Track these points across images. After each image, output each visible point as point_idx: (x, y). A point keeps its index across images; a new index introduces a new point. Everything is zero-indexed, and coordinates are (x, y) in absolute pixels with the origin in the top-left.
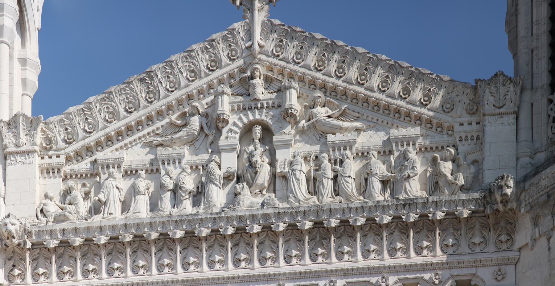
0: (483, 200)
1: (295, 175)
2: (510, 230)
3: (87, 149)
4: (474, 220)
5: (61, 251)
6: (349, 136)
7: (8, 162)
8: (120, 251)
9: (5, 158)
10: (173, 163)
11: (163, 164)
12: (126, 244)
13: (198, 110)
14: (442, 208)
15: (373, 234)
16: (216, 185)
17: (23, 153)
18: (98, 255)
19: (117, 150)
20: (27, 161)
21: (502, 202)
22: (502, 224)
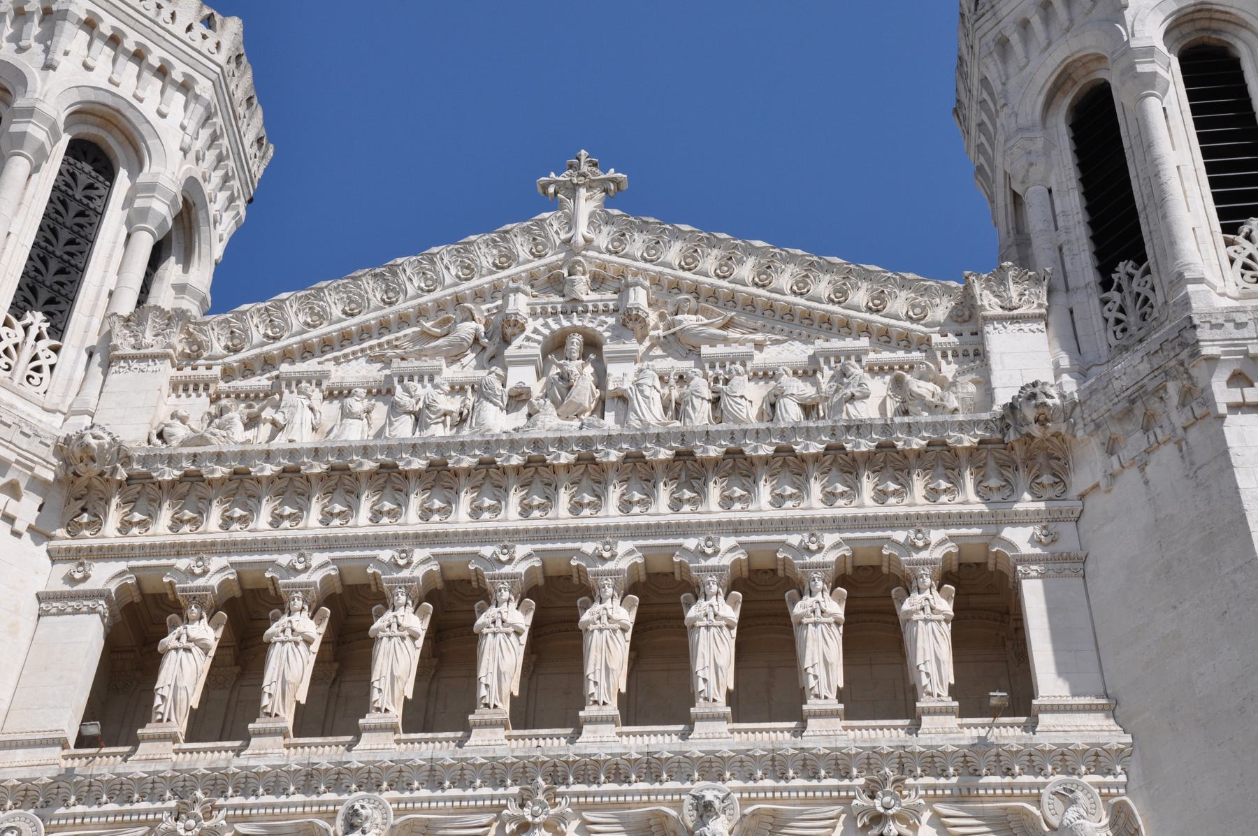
0: (998, 423)
1: (641, 392)
2: (1057, 468)
3: (266, 361)
4: (984, 455)
5: (184, 488)
7: (113, 369)
8: (300, 491)
10: (419, 381)
11: (401, 381)
12: (313, 480)
13: (472, 314)
14: (920, 432)
15: (787, 474)
16: (495, 404)
17: (144, 358)
18: (254, 497)
20: (150, 369)
21: (1037, 421)
22: (1041, 459)
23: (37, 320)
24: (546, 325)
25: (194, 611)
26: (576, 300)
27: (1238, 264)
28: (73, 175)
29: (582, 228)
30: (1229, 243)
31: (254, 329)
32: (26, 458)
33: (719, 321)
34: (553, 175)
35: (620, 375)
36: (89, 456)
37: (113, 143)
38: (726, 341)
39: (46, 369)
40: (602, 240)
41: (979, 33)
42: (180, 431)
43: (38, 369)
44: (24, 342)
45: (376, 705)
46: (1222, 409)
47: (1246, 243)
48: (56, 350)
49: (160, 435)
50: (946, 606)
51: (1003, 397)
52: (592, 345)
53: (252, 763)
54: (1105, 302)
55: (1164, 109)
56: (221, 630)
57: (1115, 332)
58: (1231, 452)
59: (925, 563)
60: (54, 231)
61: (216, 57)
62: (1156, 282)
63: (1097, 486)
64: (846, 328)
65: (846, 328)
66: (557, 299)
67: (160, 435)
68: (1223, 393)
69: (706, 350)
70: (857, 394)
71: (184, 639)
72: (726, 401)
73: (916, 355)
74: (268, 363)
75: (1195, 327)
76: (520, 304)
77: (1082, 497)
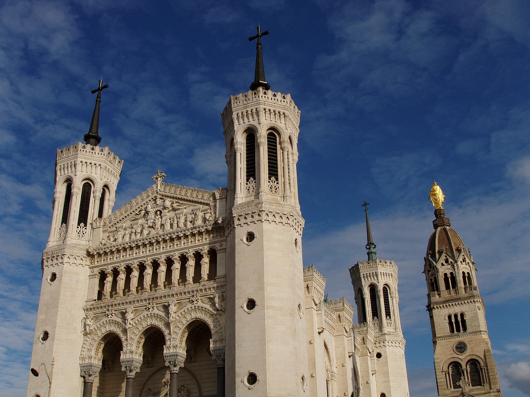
6: (181, 211)
23: (82, 224)
26: (157, 205)
27: (247, 189)
28: (84, 192)
30: (247, 184)
33: (179, 204)
34: (154, 176)
39: (85, 233)
40: (162, 190)
43: (84, 234)
44: (81, 230)
46: (236, 226)
48: (86, 229)
60: (83, 205)
64: (198, 203)
65: (198, 203)
73: (207, 207)
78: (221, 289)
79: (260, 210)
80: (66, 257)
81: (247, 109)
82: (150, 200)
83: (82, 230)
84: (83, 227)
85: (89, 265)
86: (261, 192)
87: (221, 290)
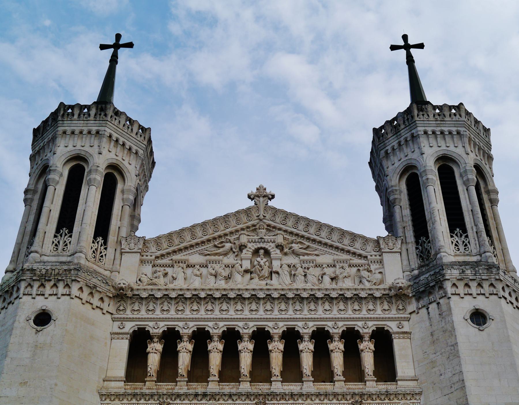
9: (122, 255)
16: (240, 274)
19: (184, 255)
23: (100, 239)
24: (253, 246)
25: (156, 340)
26: (261, 238)
29: (262, 212)
30: (452, 236)
31: (164, 243)
32: (105, 290)
33: (305, 246)
35: (276, 265)
36: (122, 289)
37: (116, 174)
38: (308, 254)
41: (380, 149)
42: (145, 279)
43: (102, 256)
44: (98, 248)
45: (212, 374)
46: (450, 296)
47: (456, 237)
48: (106, 249)
49: (140, 280)
50: (372, 347)
51: (389, 281)
52: (267, 253)
53: (179, 391)
54: (417, 248)
55: (434, 189)
56: (163, 345)
57: (420, 259)
58: (452, 309)
59: (367, 333)
61: (144, 143)
62: (432, 247)
63: (414, 311)
66: (256, 237)
67: (140, 280)
68: (450, 290)
69: (301, 257)
70: (347, 276)
71: (154, 349)
72: (308, 275)
73: (362, 261)
74: (169, 254)
75: (443, 269)
76: (244, 239)
77: (410, 313)
78: (410, 399)
79: (497, 277)
80: (78, 286)
81: (443, 128)
82: (243, 229)
83: (101, 249)
84: (101, 246)
85: (112, 314)
86: (488, 252)
87: (411, 401)
